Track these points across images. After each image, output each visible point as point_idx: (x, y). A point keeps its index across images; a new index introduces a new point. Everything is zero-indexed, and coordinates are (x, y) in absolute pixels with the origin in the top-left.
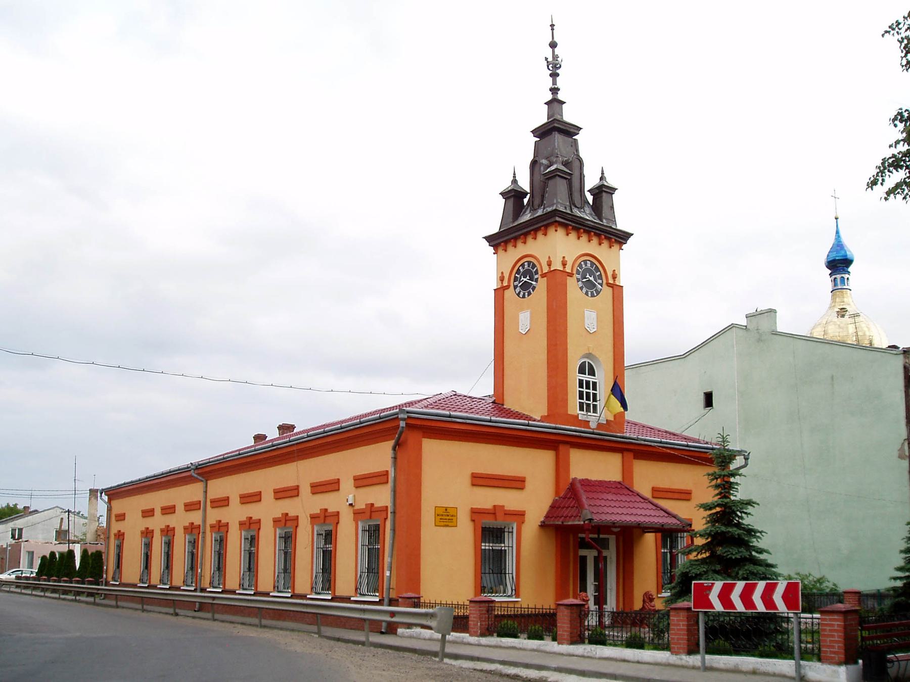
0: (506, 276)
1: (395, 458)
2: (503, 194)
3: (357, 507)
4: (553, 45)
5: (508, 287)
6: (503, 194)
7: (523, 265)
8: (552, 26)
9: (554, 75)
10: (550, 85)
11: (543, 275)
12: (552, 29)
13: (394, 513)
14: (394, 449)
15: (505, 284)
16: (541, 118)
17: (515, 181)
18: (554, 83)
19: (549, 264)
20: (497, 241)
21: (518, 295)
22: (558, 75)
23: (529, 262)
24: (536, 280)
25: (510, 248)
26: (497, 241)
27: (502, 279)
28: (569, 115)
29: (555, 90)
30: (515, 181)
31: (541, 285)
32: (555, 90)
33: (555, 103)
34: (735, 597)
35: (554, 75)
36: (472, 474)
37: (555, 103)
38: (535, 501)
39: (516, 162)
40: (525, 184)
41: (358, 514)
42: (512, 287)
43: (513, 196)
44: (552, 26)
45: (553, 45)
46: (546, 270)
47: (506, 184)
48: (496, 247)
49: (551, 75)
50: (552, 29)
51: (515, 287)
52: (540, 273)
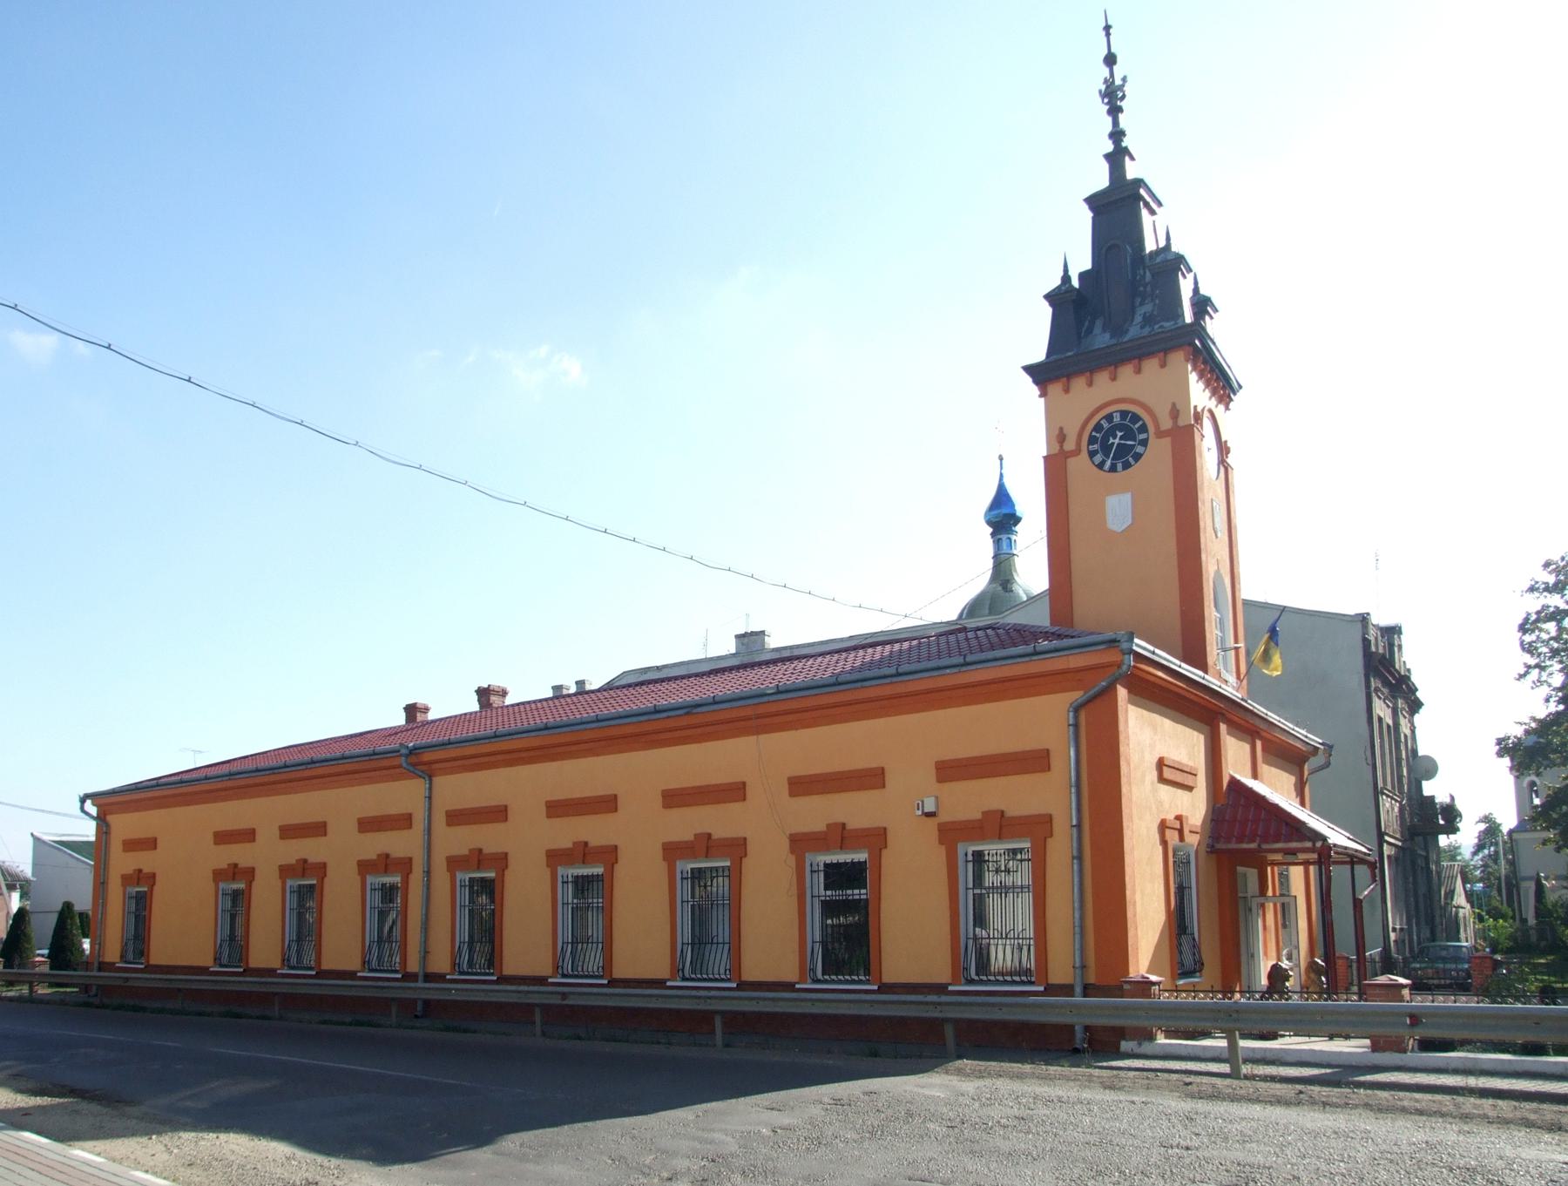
2: (1047, 297)
3: (944, 817)
4: (1110, 60)
5: (1077, 452)
6: (1047, 297)
7: (1109, 418)
8: (1107, 28)
9: (1115, 111)
10: (1109, 128)
11: (1160, 434)
12: (1108, 35)
17: (1066, 278)
18: (1116, 123)
20: (1040, 374)
21: (1100, 466)
22: (1120, 110)
23: (1124, 414)
24: (1144, 443)
25: (1079, 384)
26: (1040, 374)
29: (1117, 135)
31: (1157, 454)
32: (1117, 135)
33: (1117, 157)
35: (1115, 111)
36: (937, 763)
37: (1117, 157)
42: (1084, 454)
44: (1107, 28)
45: (1110, 60)
46: (1166, 424)
47: (1056, 282)
49: (1109, 112)
50: (1108, 35)
51: (1092, 454)
52: (1151, 429)
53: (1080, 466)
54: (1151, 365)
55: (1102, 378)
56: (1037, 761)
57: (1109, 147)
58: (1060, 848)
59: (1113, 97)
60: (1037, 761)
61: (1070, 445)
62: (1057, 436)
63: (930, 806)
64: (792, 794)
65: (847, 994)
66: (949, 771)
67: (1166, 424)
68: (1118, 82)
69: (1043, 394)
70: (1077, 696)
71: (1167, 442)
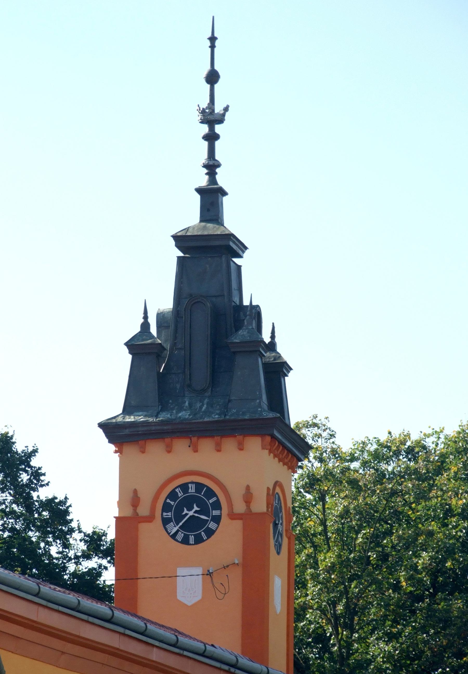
4: (212, 78)
5: (150, 519)
9: (211, 138)
10: (205, 155)
11: (233, 516)
12: (213, 47)
23: (199, 486)
24: (217, 520)
35: (211, 138)
45: (212, 78)
46: (240, 507)
50: (213, 47)
51: (166, 522)
54: (229, 445)
55: (181, 446)
59: (211, 118)
61: (143, 511)
62: (130, 497)
67: (240, 507)
68: (218, 109)
69: (119, 451)
71: (238, 524)
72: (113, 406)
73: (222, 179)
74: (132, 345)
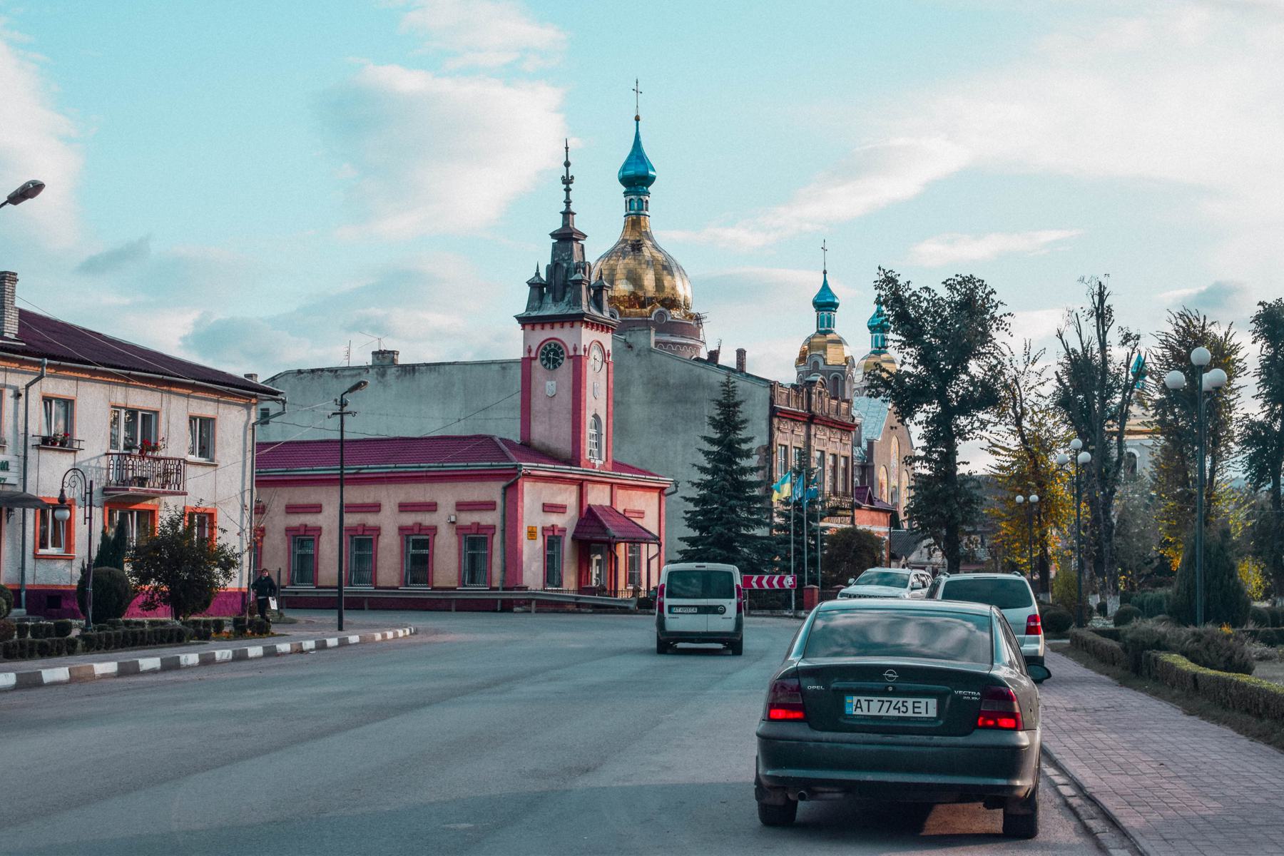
0: (534, 349)
1: (504, 494)
4: (567, 164)
5: (535, 358)
9: (568, 190)
11: (569, 357)
13: (503, 531)
14: (505, 488)
15: (533, 355)
16: (558, 224)
17: (538, 274)
18: (568, 197)
19: (575, 349)
26: (524, 321)
27: (530, 351)
28: (578, 224)
29: (568, 203)
30: (538, 274)
31: (566, 366)
32: (568, 203)
33: (567, 214)
34: (764, 582)
35: (568, 190)
37: (567, 214)
38: (566, 521)
39: (540, 256)
40: (543, 276)
41: (461, 530)
43: (536, 287)
45: (567, 164)
46: (572, 353)
48: (523, 326)
53: (537, 364)
55: (548, 327)
56: (490, 506)
57: (563, 208)
58: (497, 539)
60: (490, 506)
63: (453, 519)
64: (401, 511)
65: (419, 590)
66: (462, 507)
69: (524, 328)
70: (504, 483)
72: (521, 309)
73: (573, 208)
74: (531, 284)
